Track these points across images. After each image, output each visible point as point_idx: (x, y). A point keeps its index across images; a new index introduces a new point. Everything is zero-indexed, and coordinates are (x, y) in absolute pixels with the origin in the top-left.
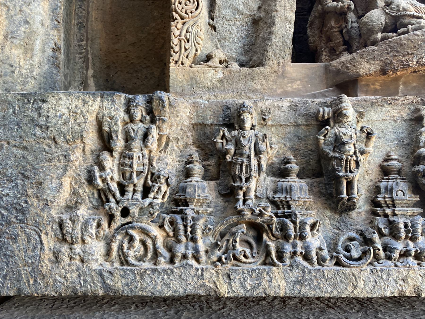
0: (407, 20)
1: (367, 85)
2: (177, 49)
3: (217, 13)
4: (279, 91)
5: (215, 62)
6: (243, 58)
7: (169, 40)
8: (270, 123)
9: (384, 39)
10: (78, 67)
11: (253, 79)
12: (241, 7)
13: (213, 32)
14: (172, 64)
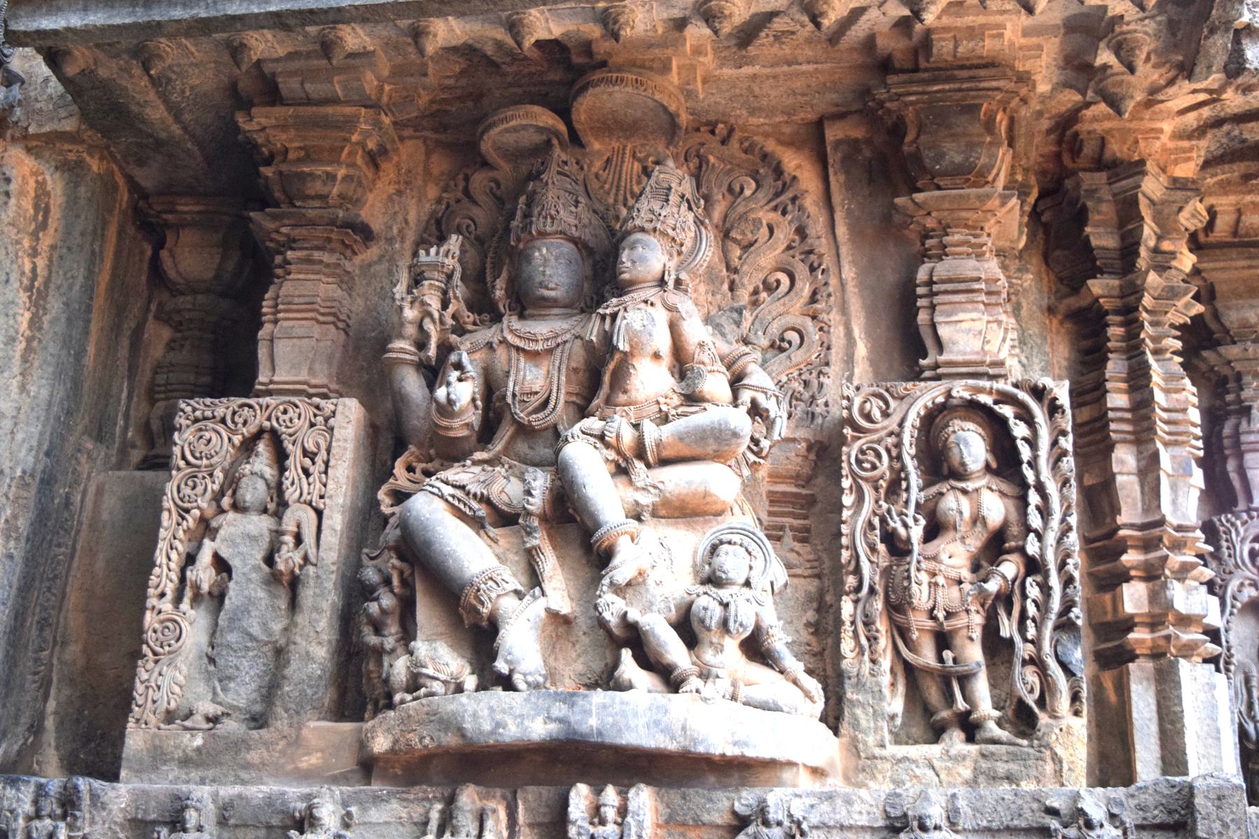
0: (422, 681)
1: (386, 769)
2: (140, 700)
3: (218, 640)
4: (290, 767)
5: (198, 721)
6: (258, 708)
7: (132, 688)
8: (232, 821)
9: (403, 702)
10: (28, 698)
11: (249, 748)
12: (256, 630)
13: (212, 668)
14: (131, 724)
